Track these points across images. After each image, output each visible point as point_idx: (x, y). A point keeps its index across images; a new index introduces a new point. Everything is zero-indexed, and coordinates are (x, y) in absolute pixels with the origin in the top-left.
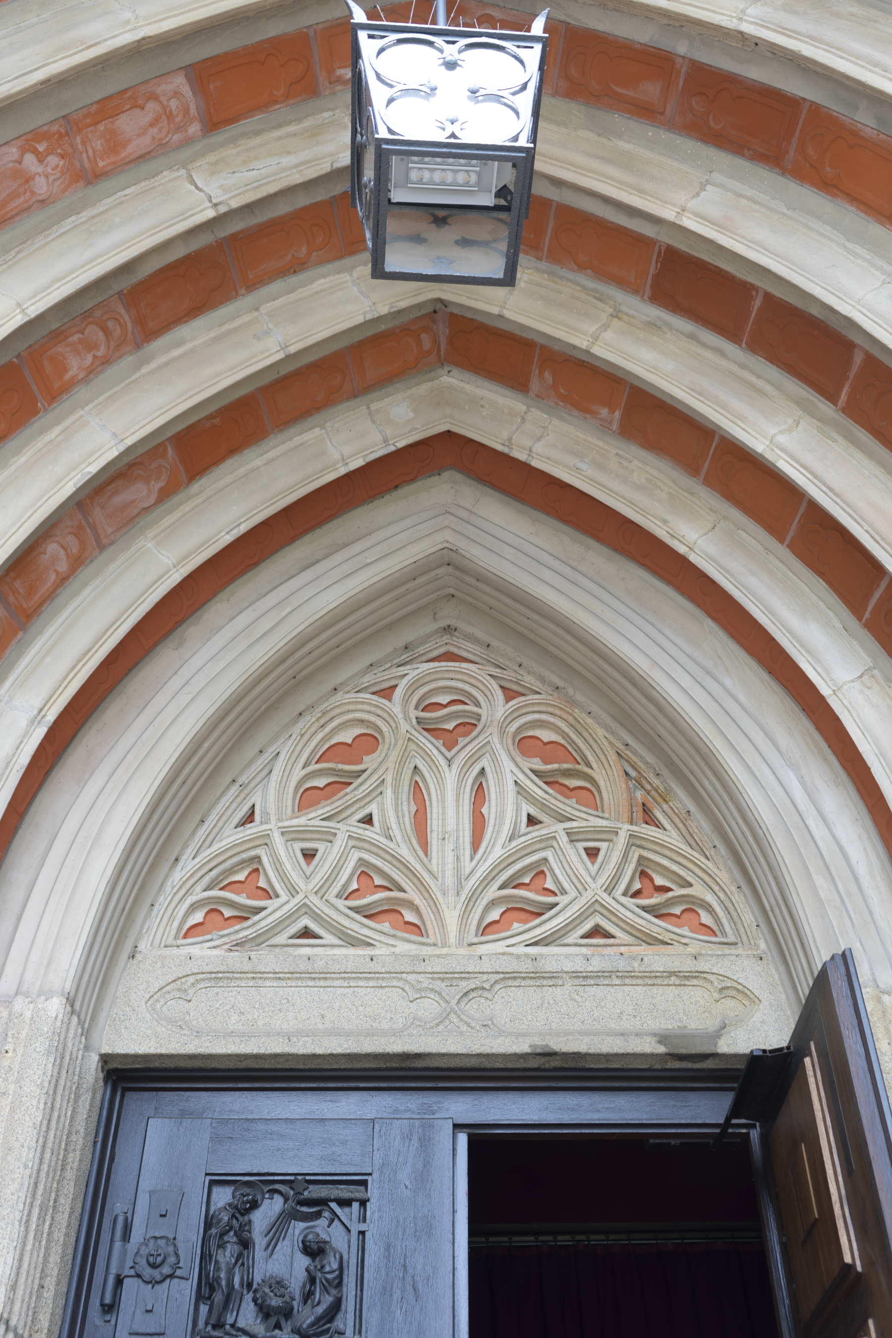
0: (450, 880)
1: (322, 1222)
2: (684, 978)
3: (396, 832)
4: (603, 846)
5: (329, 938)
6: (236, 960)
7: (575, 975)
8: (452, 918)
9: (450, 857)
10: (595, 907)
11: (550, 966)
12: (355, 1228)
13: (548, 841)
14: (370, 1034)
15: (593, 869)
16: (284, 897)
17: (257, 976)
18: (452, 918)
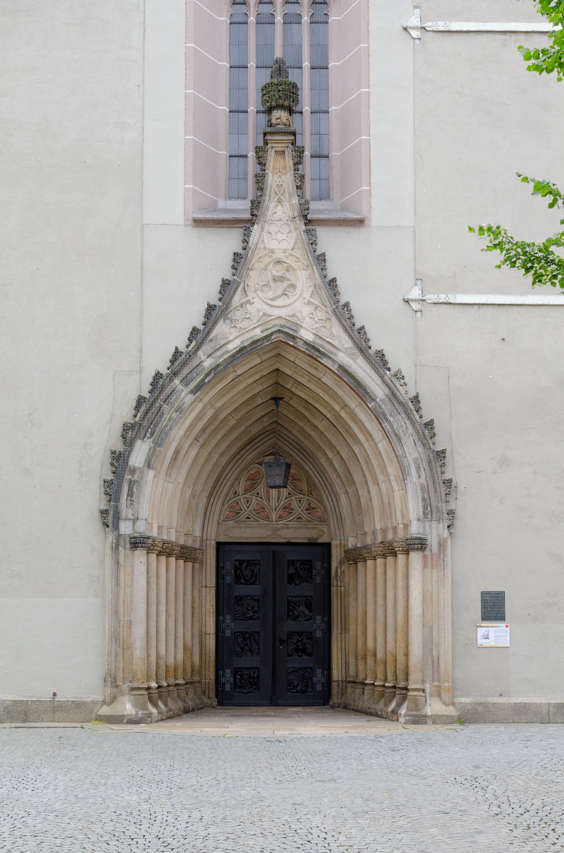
0: (274, 509)
1: (253, 567)
2: (313, 528)
3: (264, 498)
4: (302, 500)
5: (252, 519)
6: (236, 525)
7: (295, 528)
8: (274, 516)
9: (274, 503)
10: (299, 514)
11: (290, 526)
12: (258, 567)
13: (292, 500)
14: (260, 538)
15: (300, 505)
16: (243, 511)
17: (240, 527)
18: (274, 516)
